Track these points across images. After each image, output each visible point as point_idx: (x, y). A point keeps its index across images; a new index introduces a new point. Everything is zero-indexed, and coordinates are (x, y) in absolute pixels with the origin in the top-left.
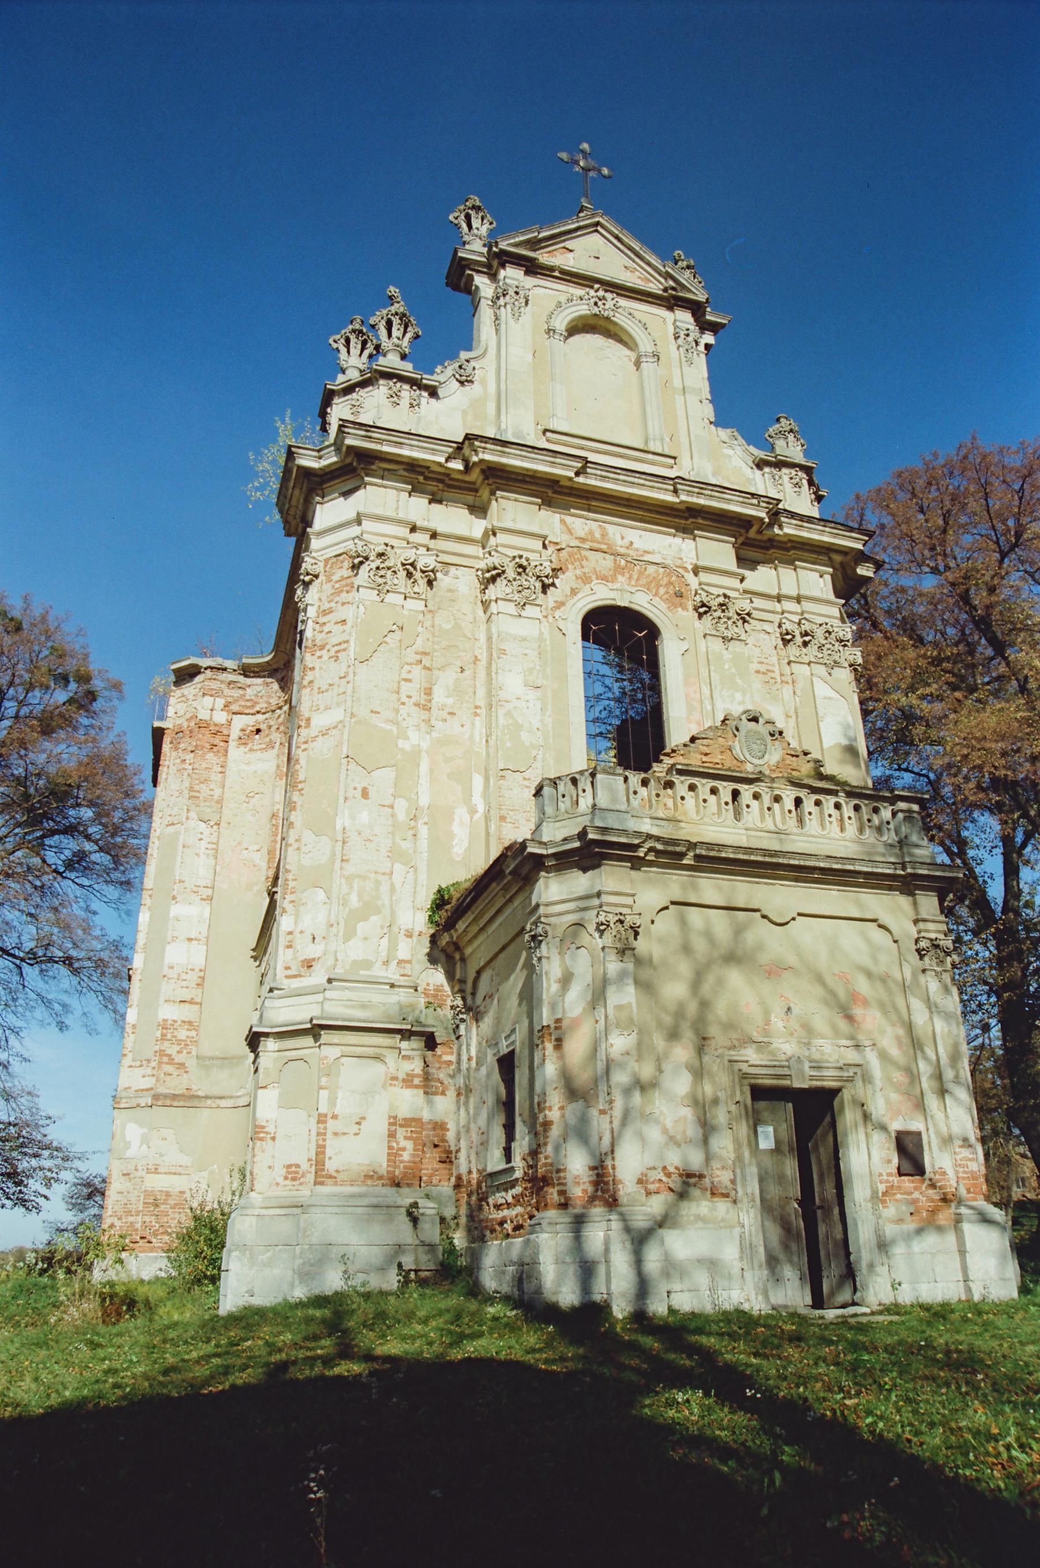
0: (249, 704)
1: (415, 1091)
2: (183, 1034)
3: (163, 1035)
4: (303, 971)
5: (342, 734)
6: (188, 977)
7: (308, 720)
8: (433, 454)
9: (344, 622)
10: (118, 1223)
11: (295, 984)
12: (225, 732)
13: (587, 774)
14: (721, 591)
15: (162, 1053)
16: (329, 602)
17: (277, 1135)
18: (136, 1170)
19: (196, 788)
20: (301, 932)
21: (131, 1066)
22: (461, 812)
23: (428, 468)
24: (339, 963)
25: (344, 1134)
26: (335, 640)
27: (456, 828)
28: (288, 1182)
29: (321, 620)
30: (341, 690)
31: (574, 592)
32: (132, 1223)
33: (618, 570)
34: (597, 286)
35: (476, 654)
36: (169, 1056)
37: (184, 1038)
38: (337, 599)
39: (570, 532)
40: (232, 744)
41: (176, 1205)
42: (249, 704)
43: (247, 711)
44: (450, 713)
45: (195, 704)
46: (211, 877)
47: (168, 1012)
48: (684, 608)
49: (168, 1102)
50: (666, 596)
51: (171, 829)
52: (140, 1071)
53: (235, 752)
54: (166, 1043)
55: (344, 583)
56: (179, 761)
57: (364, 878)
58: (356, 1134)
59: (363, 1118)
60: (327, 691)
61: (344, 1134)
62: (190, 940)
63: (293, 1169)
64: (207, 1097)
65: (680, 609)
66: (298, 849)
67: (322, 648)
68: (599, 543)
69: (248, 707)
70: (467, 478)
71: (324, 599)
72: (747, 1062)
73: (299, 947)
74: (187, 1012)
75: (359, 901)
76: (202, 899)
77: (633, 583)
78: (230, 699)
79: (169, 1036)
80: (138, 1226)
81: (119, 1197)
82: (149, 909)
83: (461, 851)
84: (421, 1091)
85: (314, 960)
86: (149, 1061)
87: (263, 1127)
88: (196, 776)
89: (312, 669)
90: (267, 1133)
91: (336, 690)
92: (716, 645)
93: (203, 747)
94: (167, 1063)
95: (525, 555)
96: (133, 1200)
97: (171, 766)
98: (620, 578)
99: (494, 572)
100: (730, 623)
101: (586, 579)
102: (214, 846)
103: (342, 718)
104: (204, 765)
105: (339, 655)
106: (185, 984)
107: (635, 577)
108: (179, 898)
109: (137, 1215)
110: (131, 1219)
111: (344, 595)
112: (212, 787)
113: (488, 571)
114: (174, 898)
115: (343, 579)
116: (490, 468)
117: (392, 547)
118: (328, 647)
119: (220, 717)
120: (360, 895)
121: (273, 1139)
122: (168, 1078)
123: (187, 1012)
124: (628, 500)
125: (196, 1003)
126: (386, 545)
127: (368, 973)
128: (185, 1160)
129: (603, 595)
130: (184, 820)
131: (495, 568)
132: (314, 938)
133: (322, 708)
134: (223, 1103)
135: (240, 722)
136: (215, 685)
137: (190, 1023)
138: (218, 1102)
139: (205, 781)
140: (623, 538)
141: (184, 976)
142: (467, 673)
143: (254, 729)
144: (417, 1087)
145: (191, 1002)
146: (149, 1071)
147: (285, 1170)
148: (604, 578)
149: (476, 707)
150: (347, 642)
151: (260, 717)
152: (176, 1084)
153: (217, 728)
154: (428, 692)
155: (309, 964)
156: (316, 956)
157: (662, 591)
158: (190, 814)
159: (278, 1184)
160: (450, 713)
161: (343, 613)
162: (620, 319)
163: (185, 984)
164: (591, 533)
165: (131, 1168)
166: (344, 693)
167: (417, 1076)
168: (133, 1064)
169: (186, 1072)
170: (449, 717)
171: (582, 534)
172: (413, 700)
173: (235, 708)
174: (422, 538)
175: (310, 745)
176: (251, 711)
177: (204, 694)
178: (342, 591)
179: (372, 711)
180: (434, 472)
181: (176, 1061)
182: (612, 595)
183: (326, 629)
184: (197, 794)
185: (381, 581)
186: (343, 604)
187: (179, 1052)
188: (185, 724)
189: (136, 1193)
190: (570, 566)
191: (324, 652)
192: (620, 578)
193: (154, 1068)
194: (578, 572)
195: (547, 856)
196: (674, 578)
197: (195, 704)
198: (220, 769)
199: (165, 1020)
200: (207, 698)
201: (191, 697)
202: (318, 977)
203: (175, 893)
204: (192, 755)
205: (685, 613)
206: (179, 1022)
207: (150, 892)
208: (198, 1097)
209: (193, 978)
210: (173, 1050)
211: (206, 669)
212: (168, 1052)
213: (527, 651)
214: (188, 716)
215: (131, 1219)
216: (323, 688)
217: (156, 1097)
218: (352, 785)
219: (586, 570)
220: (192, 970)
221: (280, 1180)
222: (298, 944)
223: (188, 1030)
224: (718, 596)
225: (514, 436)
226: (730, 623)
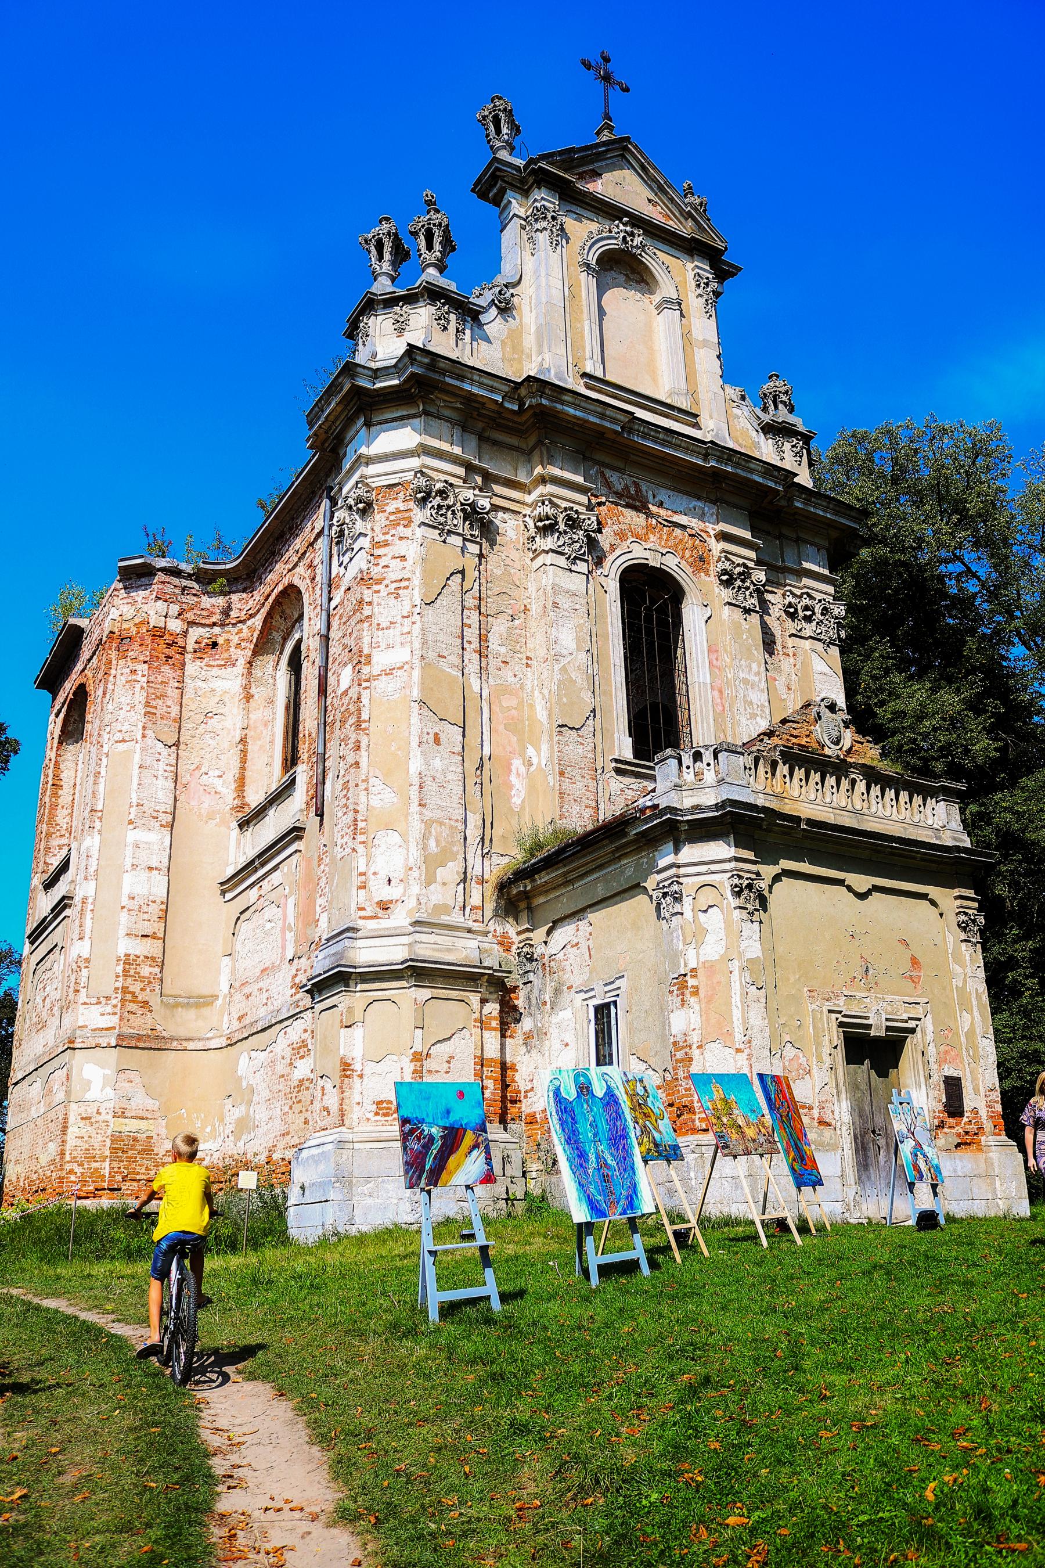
0: (204, 613)
1: (493, 1033)
2: (146, 970)
3: (124, 970)
4: (380, 913)
5: (410, 676)
6: (150, 909)
7: (369, 656)
8: (491, 392)
9: (403, 558)
10: (78, 1170)
11: (372, 924)
12: (181, 643)
13: (712, 749)
14: (741, 561)
15: (125, 990)
16: (383, 534)
17: (364, 1072)
18: (98, 1113)
19: (153, 703)
20: (375, 874)
21: (85, 1003)
22: (517, 763)
23: (483, 404)
24: (423, 906)
25: (437, 1072)
27: (513, 779)
28: (378, 1118)
29: (377, 552)
30: (406, 629)
32: (96, 1169)
33: (649, 528)
34: (625, 219)
35: (526, 602)
36: (133, 993)
37: (148, 975)
38: (393, 532)
40: (188, 657)
41: (144, 1151)
42: (204, 613)
43: (203, 622)
44: (504, 662)
45: (145, 608)
46: (171, 801)
47: (126, 946)
48: (707, 574)
49: (133, 1043)
50: (691, 560)
51: (121, 747)
52: (96, 1010)
53: (192, 667)
54: (130, 980)
55: (399, 515)
56: (128, 670)
57: (441, 824)
58: (447, 1072)
59: (452, 1057)
60: (388, 628)
61: (437, 1072)
62: (151, 869)
63: (385, 1105)
64: (172, 1039)
65: (702, 574)
66: (367, 789)
67: (379, 582)
68: (634, 500)
69: (204, 617)
70: (516, 419)
71: (377, 529)
72: (840, 1012)
73: (373, 889)
74: (152, 948)
75: (437, 846)
76: (161, 826)
77: (663, 543)
78: (184, 606)
79: (132, 972)
80: (107, 1172)
81: (79, 1142)
82: (100, 832)
83: (519, 802)
84: (498, 1033)
85: (391, 902)
86: (108, 998)
87: (350, 1065)
88: (152, 691)
89: (370, 603)
90: (352, 1070)
91: (398, 629)
92: (737, 613)
93: (158, 658)
94: (130, 1001)
95: (576, 507)
96: (97, 1146)
97: (118, 676)
98: (652, 538)
99: (547, 522)
100: (747, 593)
101: (621, 536)
102: (172, 769)
103: (408, 658)
104: (160, 679)
105: (400, 592)
106: (146, 916)
107: (665, 537)
108: (139, 823)
109: (104, 1161)
110: (94, 1165)
111: (401, 529)
112: (169, 703)
113: (540, 520)
114: (131, 822)
115: (398, 511)
116: (542, 412)
117: (451, 485)
118: (385, 582)
119: (175, 626)
120: (437, 841)
121: (361, 1076)
122: (132, 1016)
123: (152, 948)
124: (663, 459)
125: (159, 938)
126: (446, 482)
127: (448, 918)
128: (151, 1104)
130: (139, 737)
131: (548, 518)
132: (389, 880)
133: (383, 646)
134: (191, 1045)
135: (195, 633)
136: (169, 589)
137: (153, 959)
138: (185, 1044)
139: (162, 696)
140: (654, 497)
141: (145, 908)
142: (517, 622)
143: (209, 642)
144: (494, 1029)
145: (154, 937)
146: (109, 1009)
147: (375, 1106)
149: (528, 658)
150: (408, 579)
151: (217, 630)
152: (141, 1024)
153: (172, 638)
155: (385, 906)
156: (394, 897)
157: (688, 554)
158: (147, 732)
159: (368, 1119)
160: (504, 662)
161: (400, 547)
162: (646, 259)
163: (146, 916)
164: (627, 488)
165: (91, 1110)
166: (409, 633)
167: (494, 1018)
168: (88, 1001)
169: (151, 1011)
170: (503, 665)
171: (619, 487)
172: (473, 646)
173: (190, 616)
175: (375, 683)
176: (208, 622)
177: (158, 598)
178: (399, 524)
179: (439, 656)
180: (487, 409)
181: (140, 998)
182: (647, 554)
183: (383, 562)
184: (154, 711)
185: (442, 519)
186: (401, 538)
187: (142, 990)
188: (134, 630)
189: (100, 1138)
190: (609, 521)
191: (381, 587)
192: (652, 538)
193: (115, 1006)
194: (616, 527)
195: (683, 822)
196: (697, 542)
197: (145, 608)
198: (177, 684)
199: (127, 955)
200: (160, 602)
201: (139, 599)
202: (400, 918)
203: (132, 817)
204: (146, 666)
205: (707, 579)
206: (142, 958)
207: (100, 814)
208: (163, 1037)
209: (155, 910)
210: (136, 988)
211: (159, 570)
212: (131, 989)
213: (577, 607)
214: (137, 620)
215: (94, 1165)
216: (384, 625)
218: (425, 730)
219: (623, 527)
220: (154, 902)
221: (371, 1115)
222: (373, 883)
223: (151, 966)
224: (738, 565)
225: (556, 376)
226: (747, 593)
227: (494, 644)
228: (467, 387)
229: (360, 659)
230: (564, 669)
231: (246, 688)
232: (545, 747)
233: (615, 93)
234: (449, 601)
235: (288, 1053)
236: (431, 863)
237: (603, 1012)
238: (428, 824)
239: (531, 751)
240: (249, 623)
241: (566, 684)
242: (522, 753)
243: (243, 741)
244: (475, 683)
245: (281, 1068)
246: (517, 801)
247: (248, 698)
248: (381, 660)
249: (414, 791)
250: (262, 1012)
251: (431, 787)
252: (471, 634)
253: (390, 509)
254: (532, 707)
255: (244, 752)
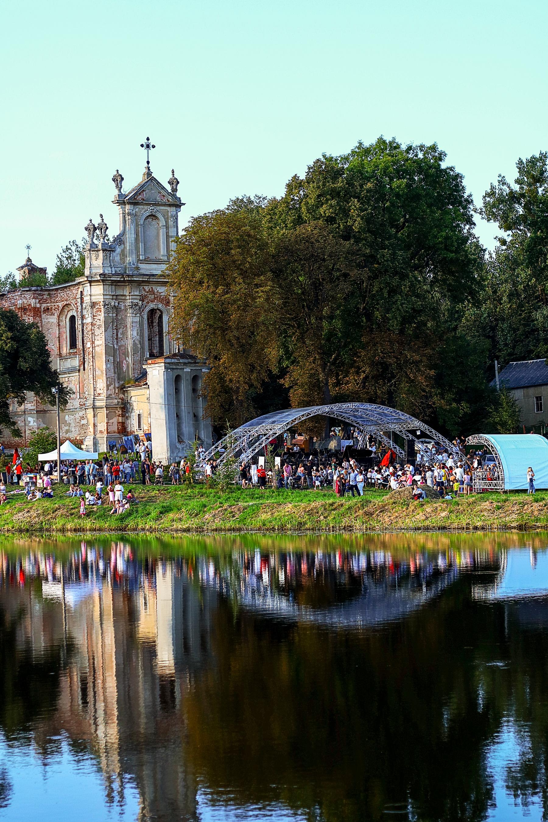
9: (100, 320)
11: (97, 398)
22: (124, 361)
26: (98, 324)
31: (146, 306)
39: (145, 290)
53: (43, 316)
101: (148, 303)
115: (98, 308)
119: (38, 305)
129: (152, 306)
134: (52, 412)
136: (36, 295)
148: (152, 302)
151: (49, 305)
154: (117, 335)
155: (99, 394)
161: (99, 317)
171: (147, 290)
174: (115, 297)
183: (96, 320)
217: (37, 411)
227: (120, 336)
228: (112, 279)
229: (93, 343)
230: (134, 341)
231: (59, 322)
232: (130, 358)
233: (152, 150)
234: (110, 330)
235: (79, 418)
236: (108, 386)
237: (139, 415)
238: (107, 378)
239: (127, 358)
240: (57, 304)
241: (135, 344)
242: (126, 359)
243: (59, 337)
244: (115, 346)
245: (77, 420)
246: (124, 370)
247: (59, 325)
248: (97, 343)
249: (104, 372)
250: (72, 408)
251: (108, 371)
252: (115, 335)
253: (96, 307)
254: (128, 349)
255: (59, 340)
